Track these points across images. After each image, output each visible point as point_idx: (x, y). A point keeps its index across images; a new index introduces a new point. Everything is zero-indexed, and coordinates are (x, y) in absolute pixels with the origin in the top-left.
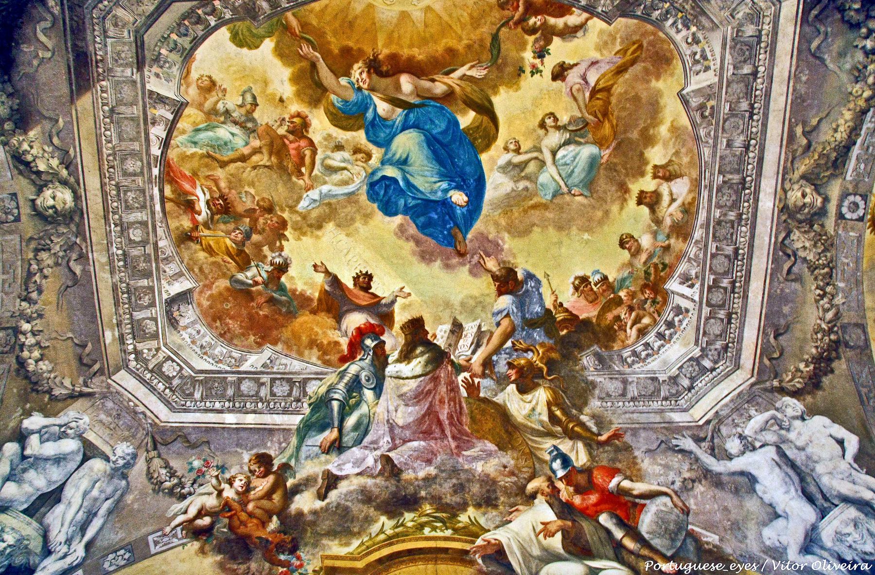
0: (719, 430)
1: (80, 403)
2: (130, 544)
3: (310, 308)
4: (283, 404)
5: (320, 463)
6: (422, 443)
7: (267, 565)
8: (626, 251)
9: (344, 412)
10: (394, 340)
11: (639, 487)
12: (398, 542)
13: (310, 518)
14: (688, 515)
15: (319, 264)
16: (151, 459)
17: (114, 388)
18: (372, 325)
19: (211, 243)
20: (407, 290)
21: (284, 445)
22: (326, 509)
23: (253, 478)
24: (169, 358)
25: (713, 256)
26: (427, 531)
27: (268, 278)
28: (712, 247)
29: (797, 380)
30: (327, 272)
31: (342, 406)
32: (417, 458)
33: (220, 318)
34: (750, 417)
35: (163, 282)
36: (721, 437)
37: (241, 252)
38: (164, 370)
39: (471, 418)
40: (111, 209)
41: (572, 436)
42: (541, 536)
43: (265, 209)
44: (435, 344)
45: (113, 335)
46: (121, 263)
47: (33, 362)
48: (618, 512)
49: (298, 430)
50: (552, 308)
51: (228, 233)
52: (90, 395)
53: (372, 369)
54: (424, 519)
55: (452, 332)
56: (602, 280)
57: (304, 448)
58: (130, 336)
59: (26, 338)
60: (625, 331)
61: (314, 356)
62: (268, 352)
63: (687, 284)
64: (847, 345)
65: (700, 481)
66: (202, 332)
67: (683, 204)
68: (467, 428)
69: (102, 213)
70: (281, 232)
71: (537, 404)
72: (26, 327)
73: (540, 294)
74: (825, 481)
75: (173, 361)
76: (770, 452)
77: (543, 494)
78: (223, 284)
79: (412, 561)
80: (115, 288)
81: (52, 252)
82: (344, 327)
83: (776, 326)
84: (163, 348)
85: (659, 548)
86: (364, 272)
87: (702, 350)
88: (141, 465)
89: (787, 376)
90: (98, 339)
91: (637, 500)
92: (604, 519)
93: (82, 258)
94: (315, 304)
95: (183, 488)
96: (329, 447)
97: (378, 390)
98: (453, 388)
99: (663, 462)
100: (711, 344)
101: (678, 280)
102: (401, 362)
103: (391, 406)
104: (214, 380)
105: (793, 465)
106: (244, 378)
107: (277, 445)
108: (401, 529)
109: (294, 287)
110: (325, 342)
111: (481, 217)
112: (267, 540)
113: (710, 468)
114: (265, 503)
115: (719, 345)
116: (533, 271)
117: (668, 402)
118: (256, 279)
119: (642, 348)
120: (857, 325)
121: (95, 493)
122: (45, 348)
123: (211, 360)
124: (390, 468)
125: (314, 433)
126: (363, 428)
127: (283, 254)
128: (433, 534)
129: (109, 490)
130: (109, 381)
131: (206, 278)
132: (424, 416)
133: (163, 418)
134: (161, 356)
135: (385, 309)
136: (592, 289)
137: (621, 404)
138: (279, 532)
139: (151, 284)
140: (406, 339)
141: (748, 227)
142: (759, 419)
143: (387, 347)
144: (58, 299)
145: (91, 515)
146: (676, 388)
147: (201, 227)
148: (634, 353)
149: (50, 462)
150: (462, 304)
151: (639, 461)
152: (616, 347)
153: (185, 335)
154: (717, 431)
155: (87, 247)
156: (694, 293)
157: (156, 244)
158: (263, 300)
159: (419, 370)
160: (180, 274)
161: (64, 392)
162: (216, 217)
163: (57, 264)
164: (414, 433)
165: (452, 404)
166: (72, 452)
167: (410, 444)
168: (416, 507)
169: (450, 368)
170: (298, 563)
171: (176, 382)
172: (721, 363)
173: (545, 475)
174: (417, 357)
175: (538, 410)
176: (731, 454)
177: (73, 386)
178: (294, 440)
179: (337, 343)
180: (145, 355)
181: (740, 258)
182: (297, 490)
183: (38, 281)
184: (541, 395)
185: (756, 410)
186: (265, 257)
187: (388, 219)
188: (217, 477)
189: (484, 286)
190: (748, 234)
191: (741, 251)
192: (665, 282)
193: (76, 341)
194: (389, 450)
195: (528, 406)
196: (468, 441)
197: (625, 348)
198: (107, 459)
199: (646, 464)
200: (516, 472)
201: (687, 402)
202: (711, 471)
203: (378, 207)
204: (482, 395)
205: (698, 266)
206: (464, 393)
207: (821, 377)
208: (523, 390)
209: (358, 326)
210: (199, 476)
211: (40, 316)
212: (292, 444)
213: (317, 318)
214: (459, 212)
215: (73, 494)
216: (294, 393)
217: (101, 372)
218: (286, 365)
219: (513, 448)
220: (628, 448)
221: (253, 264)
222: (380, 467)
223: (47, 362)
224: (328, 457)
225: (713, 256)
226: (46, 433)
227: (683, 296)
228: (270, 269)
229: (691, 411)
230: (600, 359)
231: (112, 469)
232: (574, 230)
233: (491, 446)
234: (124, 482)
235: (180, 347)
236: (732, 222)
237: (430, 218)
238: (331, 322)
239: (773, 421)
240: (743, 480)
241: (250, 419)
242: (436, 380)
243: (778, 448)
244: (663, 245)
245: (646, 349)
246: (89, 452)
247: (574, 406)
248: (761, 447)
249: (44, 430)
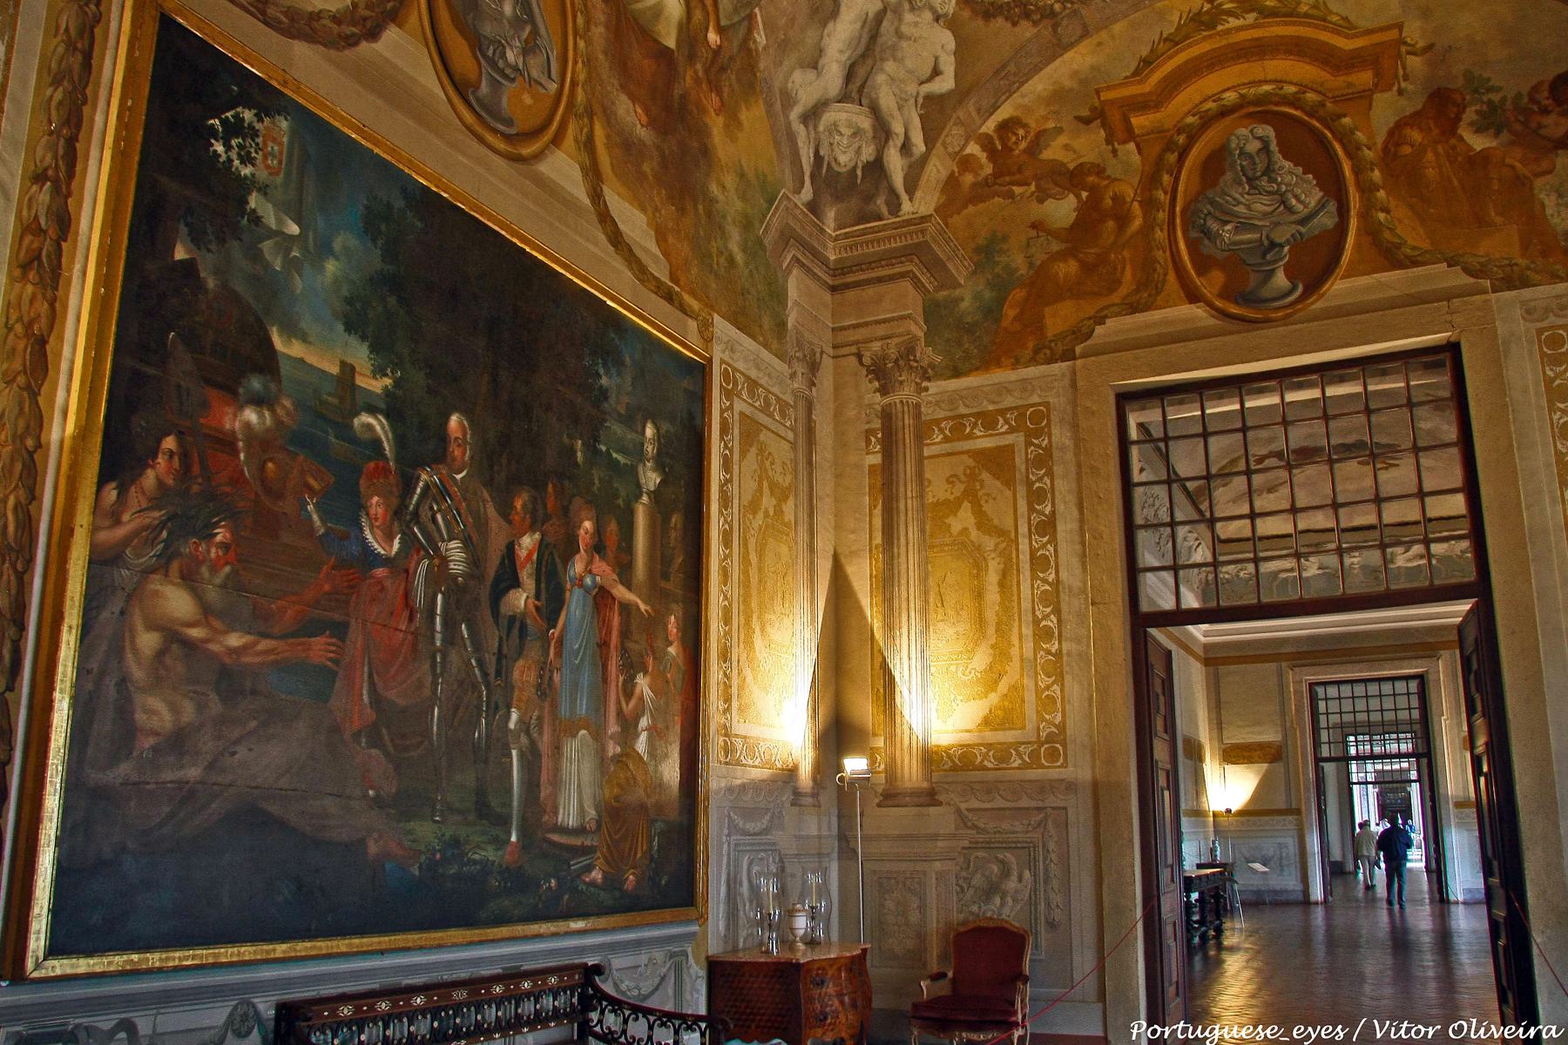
64: (1055, 27)
105: (874, 37)
120: (1085, 26)
207: (1001, 14)
243: (884, 11)
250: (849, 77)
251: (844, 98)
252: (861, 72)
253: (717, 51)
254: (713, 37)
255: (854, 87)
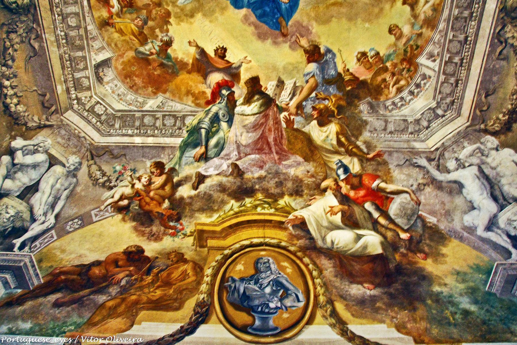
0: (443, 155)
1: (45, 132)
2: (81, 215)
3: (186, 70)
4: (170, 131)
5: (194, 168)
6: (258, 156)
7: (162, 228)
8: (393, 36)
9: (209, 135)
10: (240, 91)
11: (390, 187)
12: (241, 216)
13: (188, 201)
14: (419, 205)
15: (192, 41)
16: (90, 165)
17: (65, 122)
18: (226, 81)
19: (122, 27)
20: (249, 58)
21: (171, 156)
22: (198, 196)
23: (153, 177)
24: (98, 103)
25: (450, 41)
26: (259, 209)
27: (160, 50)
28: (450, 35)
29: (496, 125)
30: (197, 46)
31: (208, 132)
32: (254, 165)
33: (130, 77)
34: (464, 147)
35: (92, 53)
36: (444, 159)
37: (141, 33)
38: (95, 110)
39: (288, 141)
40: (54, 4)
41: (351, 154)
42: (329, 214)
43: (156, 4)
44: (267, 94)
45: (62, 89)
46: (64, 41)
47: (14, 106)
48: (377, 202)
49: (180, 147)
50: (342, 72)
51: (133, 20)
52: (51, 126)
53: (226, 109)
54: (258, 202)
55: (277, 86)
56: (376, 55)
57: (184, 158)
58: (73, 89)
59: (8, 91)
60: (389, 89)
61: (189, 100)
62: (160, 98)
63: (431, 59)
65: (429, 185)
66: (118, 86)
67: (434, 5)
68: (285, 147)
69: (49, 7)
70: (167, 19)
71: (330, 133)
72: (7, 83)
73: (335, 63)
74: (506, 189)
75: (101, 104)
76: (474, 170)
77: (331, 189)
78: (131, 54)
79: (250, 227)
80: (61, 58)
81: (19, 33)
82: (208, 82)
83: (487, 89)
84: (94, 96)
85: (400, 224)
86: (221, 46)
87: (438, 103)
88: (84, 169)
89: (490, 122)
90: (53, 91)
91: (389, 195)
92: (368, 206)
93: (38, 37)
94: (190, 67)
95: (111, 183)
96: (200, 158)
97: (230, 122)
98: (277, 122)
99: (407, 173)
100: (443, 100)
101: (426, 57)
102: (245, 105)
103: (238, 133)
104: (127, 116)
105: (487, 178)
106: (147, 115)
107: (167, 156)
108: (243, 208)
109: (176, 56)
110: (197, 92)
111: (298, 11)
112: (162, 214)
113: (435, 178)
114: (161, 192)
115: (448, 100)
116: (331, 47)
117: (413, 136)
118: (152, 51)
119: (398, 100)
121: (58, 186)
122: (20, 97)
123: (124, 103)
124: (237, 171)
125: (190, 149)
126: (220, 146)
127: (169, 34)
128: (263, 211)
129: (66, 184)
130: (62, 117)
131: (120, 50)
132: (259, 139)
133: (96, 140)
134: (93, 101)
135: (234, 71)
136: (368, 61)
137: (383, 135)
138: (169, 209)
139: (84, 55)
140: (248, 90)
141: (476, 22)
142: (469, 148)
143: (236, 95)
144: (25, 65)
145: (57, 199)
146: (419, 127)
147: (114, 17)
148: (394, 103)
149: (30, 168)
150: (284, 68)
151: (392, 171)
152: (382, 98)
153: (108, 87)
154: (442, 155)
155: (41, 30)
156: (435, 65)
157: (86, 28)
158: (157, 64)
159: (256, 110)
160: (103, 48)
161: (34, 124)
162: (124, 10)
163: (22, 42)
164: (252, 150)
165: (276, 132)
166: (43, 161)
167: (249, 157)
168: (253, 195)
169: (275, 109)
170: (181, 227)
171: (103, 118)
172: (449, 112)
173: (333, 177)
174: (255, 102)
175: (331, 137)
176: (449, 170)
177: (40, 120)
178: (178, 154)
179: (204, 93)
180: (83, 101)
181: (468, 43)
182: (180, 184)
183: (11, 53)
184: (333, 128)
185: (468, 143)
186: (157, 36)
187: (237, 11)
188: (131, 176)
189: (299, 56)
190: (476, 27)
191: (469, 39)
192: (417, 58)
193: (40, 92)
194: (237, 160)
195: (325, 135)
196: (286, 155)
197: (387, 99)
198: (64, 166)
199: (396, 173)
200: (315, 175)
201: (424, 136)
202: (436, 180)
203: (231, 3)
204: (295, 127)
205: (440, 47)
206: (284, 125)
207: (512, 123)
208: (321, 124)
209: (217, 81)
210: (120, 176)
211: (15, 76)
212: (176, 155)
213: (191, 76)
214: (283, 7)
215: (45, 186)
216: (177, 124)
217: (56, 111)
218: (172, 106)
219: (314, 161)
220: (385, 163)
221: (149, 41)
222: (231, 170)
223: (22, 106)
224: (199, 164)
225: (450, 41)
226: (26, 150)
227: (428, 67)
228: (160, 44)
229: (427, 142)
230: (372, 106)
231: (68, 172)
232: (359, 21)
233: (300, 159)
234: (75, 180)
235: (105, 95)
236: (466, 18)
237: (265, 11)
238: (200, 79)
239: (478, 150)
240: (455, 186)
241: (150, 141)
242: (266, 116)
244: (418, 32)
245: (401, 101)
246: (53, 161)
247: (353, 135)
248: (469, 166)
249: (25, 148)
250: (495, 199)
251: (502, 208)
252: (497, 193)
253: (411, 239)
254: (404, 236)
255: (501, 201)
